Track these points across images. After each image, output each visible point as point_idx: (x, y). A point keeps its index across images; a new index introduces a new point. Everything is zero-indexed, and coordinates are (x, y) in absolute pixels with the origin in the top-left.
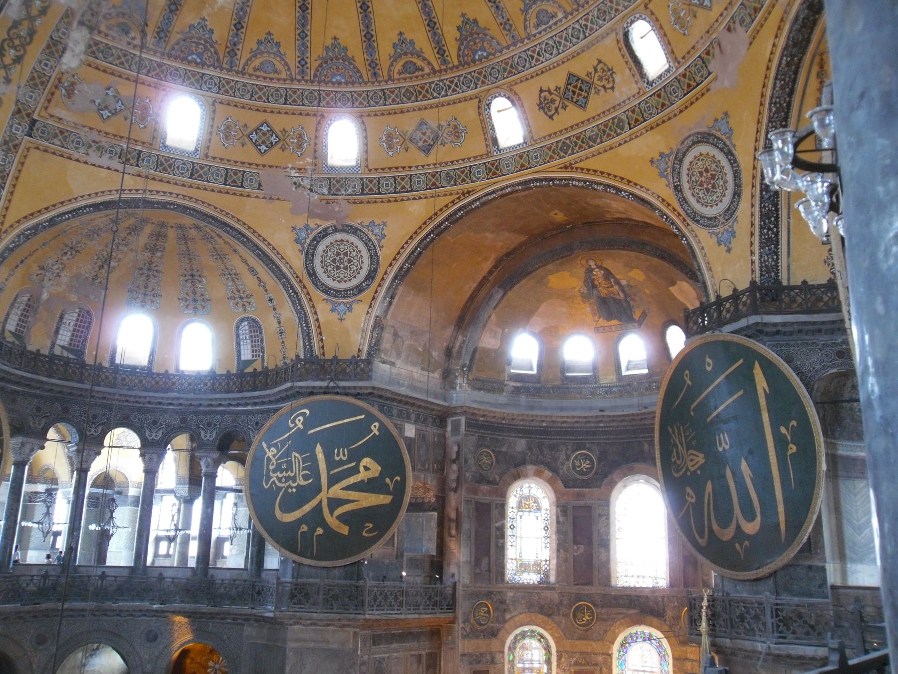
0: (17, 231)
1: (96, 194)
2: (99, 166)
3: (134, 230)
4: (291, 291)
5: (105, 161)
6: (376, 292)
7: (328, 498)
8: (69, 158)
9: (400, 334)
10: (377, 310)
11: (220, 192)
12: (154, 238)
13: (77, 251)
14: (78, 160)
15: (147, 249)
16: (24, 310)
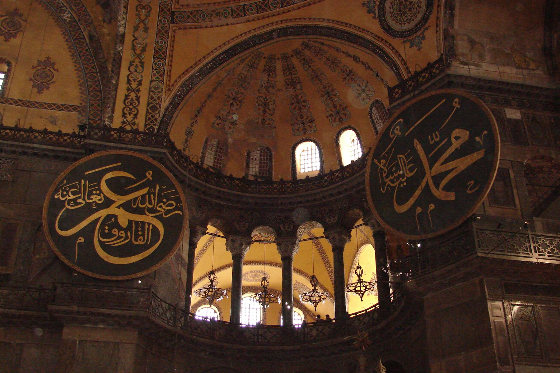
0: (180, 83)
1: (224, 44)
2: (221, 26)
3: (270, 71)
4: (378, 50)
5: (224, 21)
6: (438, 12)
7: (434, 178)
8: (201, 28)
9: (477, 40)
10: (442, 26)
11: (304, 6)
12: (288, 73)
13: (240, 101)
14: (206, 27)
15: (288, 85)
16: (217, 151)
